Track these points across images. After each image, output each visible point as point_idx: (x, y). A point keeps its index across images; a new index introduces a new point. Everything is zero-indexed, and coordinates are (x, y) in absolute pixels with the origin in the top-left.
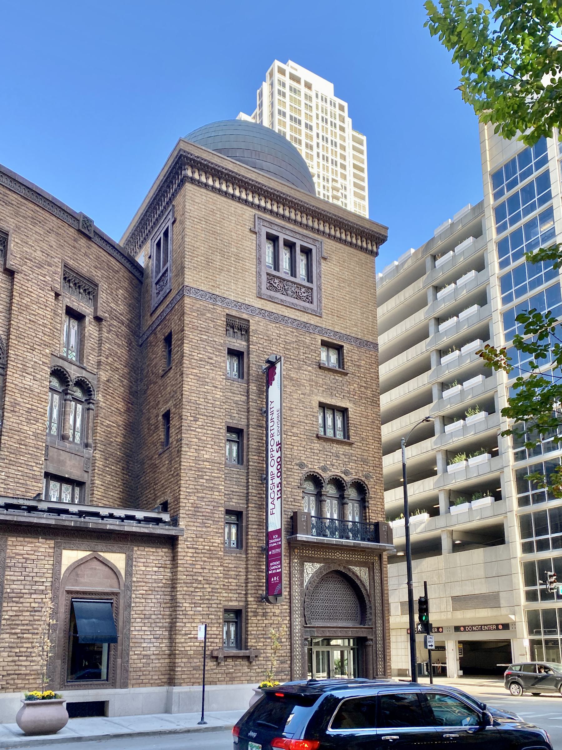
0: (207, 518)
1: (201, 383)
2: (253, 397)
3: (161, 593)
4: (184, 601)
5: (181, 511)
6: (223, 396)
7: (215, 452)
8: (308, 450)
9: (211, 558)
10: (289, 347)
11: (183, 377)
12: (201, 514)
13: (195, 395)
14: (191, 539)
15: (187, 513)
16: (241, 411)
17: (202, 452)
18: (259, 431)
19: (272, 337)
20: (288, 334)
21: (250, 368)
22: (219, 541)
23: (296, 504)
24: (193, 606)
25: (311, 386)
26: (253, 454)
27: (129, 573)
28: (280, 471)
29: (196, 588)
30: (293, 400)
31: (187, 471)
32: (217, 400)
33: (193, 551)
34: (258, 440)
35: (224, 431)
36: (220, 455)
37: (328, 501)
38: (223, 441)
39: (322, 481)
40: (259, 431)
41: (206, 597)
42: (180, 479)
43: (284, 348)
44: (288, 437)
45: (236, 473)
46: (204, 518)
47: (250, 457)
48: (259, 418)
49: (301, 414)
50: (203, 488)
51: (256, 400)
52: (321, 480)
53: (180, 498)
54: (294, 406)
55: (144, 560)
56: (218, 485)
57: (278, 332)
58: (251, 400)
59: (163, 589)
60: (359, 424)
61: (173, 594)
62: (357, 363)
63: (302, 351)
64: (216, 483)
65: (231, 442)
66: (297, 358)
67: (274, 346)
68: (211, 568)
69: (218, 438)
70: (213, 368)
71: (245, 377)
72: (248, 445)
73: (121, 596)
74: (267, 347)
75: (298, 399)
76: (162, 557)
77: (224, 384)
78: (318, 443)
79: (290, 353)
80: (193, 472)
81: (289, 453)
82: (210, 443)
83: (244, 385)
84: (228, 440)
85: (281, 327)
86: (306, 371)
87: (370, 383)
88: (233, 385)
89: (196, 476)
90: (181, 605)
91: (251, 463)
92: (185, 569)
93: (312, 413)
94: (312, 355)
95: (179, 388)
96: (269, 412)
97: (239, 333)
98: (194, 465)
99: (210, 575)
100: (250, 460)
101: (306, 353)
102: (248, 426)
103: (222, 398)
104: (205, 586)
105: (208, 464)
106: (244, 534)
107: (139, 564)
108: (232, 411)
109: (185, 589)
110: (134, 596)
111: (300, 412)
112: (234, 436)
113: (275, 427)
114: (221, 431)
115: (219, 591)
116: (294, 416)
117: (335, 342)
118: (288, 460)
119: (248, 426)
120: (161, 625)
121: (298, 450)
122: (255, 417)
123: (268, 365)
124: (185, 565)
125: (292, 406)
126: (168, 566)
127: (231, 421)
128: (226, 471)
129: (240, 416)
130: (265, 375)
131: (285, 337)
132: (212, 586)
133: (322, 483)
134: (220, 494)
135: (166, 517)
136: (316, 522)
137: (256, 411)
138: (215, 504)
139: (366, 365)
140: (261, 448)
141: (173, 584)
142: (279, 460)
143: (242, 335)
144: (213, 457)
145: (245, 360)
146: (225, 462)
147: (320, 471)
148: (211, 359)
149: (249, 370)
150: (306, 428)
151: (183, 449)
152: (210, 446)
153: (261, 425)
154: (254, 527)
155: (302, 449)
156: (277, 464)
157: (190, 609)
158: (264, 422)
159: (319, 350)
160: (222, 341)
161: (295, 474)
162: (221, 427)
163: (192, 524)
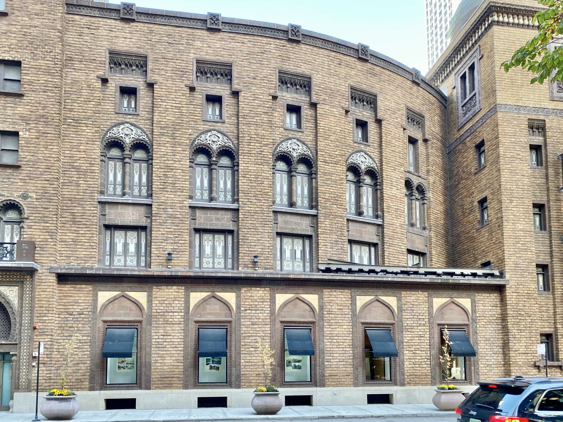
3: (495, 324)
5: (506, 268)
6: (529, 181)
7: (527, 224)
9: (529, 299)
13: (509, 184)
14: (514, 287)
17: (517, 225)
22: (534, 287)
27: (474, 311)
29: (520, 319)
33: (517, 294)
35: (531, 207)
51: (554, 181)
55: (482, 302)
59: (496, 321)
61: (504, 324)
64: (529, 245)
71: (544, 165)
72: (550, 216)
73: (471, 326)
80: (512, 240)
89: (514, 242)
97: (537, 131)
99: (529, 310)
102: (549, 201)
104: (527, 318)
107: (480, 305)
109: (513, 320)
110: (478, 326)
115: (536, 321)
119: (549, 201)
120: (497, 344)
132: (531, 318)
135: (497, 273)
137: (554, 189)
138: (529, 261)
141: (504, 318)
143: (539, 132)
145: (543, 151)
151: (504, 224)
154: (558, 275)
157: (517, 334)
160: (526, 140)
163: (514, 276)
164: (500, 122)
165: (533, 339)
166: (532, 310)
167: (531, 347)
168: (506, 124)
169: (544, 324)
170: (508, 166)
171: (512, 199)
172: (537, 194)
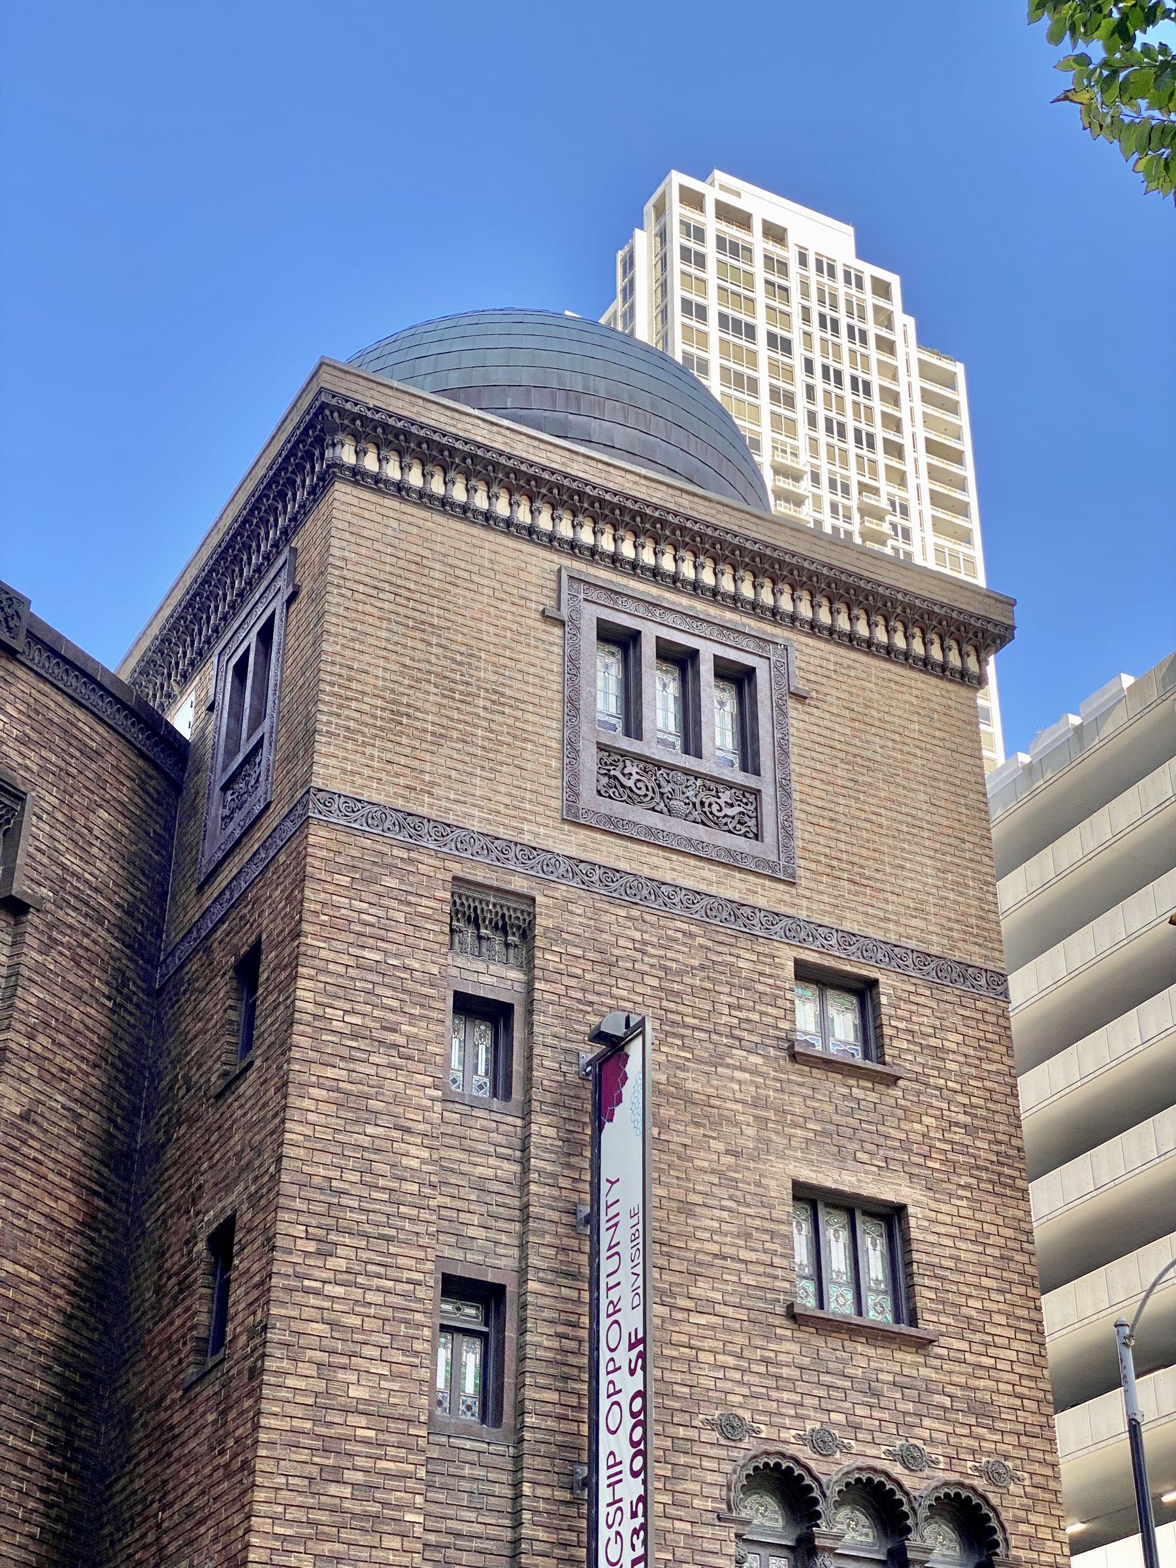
1: (350, 1115)
2: (542, 1164)
6: (433, 1162)
7: (393, 1377)
8: (755, 1368)
11: (285, 1096)
13: (328, 1159)
16: (497, 1218)
17: (341, 1375)
18: (565, 1292)
19: (616, 952)
20: (676, 940)
21: (536, 1061)
25: (762, 1122)
26: (541, 1381)
28: (640, 1449)
30: (694, 1175)
31: (279, 1452)
32: (407, 1175)
34: (561, 1329)
35: (430, 1291)
36: (412, 1387)
38: (427, 1332)
39: (816, 1494)
40: (565, 1292)
42: (253, 1485)
43: (661, 989)
45: (474, 1457)
47: (529, 1393)
48: (566, 1241)
49: (725, 1227)
50: (337, 1518)
51: (554, 1175)
52: (809, 1488)
54: (698, 1199)
56: (398, 1507)
58: (534, 1176)
60: (951, 1264)
62: (933, 1042)
63: (725, 999)
64: (392, 1497)
65: (459, 1337)
66: (705, 1025)
67: (621, 983)
69: (406, 1322)
71: (517, 1094)
72: (521, 1347)
75: (713, 1172)
77: (436, 1118)
78: (793, 1340)
79: (681, 1008)
80: (304, 1455)
81: (679, 1377)
82: (374, 1338)
83: (510, 1119)
84: (444, 1328)
85: (647, 917)
86: (742, 1069)
88: (471, 1123)
89: (315, 1471)
91: (529, 1420)
93: (768, 1225)
94: (762, 1013)
95: (272, 1133)
96: (603, 1218)
97: (498, 939)
98: (308, 1425)
100: (529, 1405)
101: (739, 1008)
102: (522, 1273)
103: (425, 1168)
105: (362, 1421)
111: (721, 1221)
112: (470, 1316)
113: (625, 1276)
114: (421, 1292)
116: (699, 1234)
117: (848, 968)
118: (677, 1405)
119: (522, 1273)
121: (716, 1366)
122: (548, 1239)
123: (599, 1048)
125: (692, 1198)
127: (459, 1255)
129: (492, 1235)
130: (590, 1086)
131: (662, 952)
133: (816, 1502)
137: (555, 1216)
139: (963, 1049)
140: (572, 1360)
143: (507, 945)
144: (384, 1395)
145: (518, 1034)
146: (431, 1415)
147: (805, 1453)
148: (394, 1031)
150: (746, 1279)
151: (270, 1364)
152: (375, 1353)
153: (573, 1269)
155: (730, 1361)
156: (629, 1422)
158: (584, 1259)
159: (789, 995)
160: (435, 970)
161: (706, 1464)
164: (314, 867)
168: (345, 881)
170: (330, 1072)
171: (333, 1237)
172: (472, 1232)
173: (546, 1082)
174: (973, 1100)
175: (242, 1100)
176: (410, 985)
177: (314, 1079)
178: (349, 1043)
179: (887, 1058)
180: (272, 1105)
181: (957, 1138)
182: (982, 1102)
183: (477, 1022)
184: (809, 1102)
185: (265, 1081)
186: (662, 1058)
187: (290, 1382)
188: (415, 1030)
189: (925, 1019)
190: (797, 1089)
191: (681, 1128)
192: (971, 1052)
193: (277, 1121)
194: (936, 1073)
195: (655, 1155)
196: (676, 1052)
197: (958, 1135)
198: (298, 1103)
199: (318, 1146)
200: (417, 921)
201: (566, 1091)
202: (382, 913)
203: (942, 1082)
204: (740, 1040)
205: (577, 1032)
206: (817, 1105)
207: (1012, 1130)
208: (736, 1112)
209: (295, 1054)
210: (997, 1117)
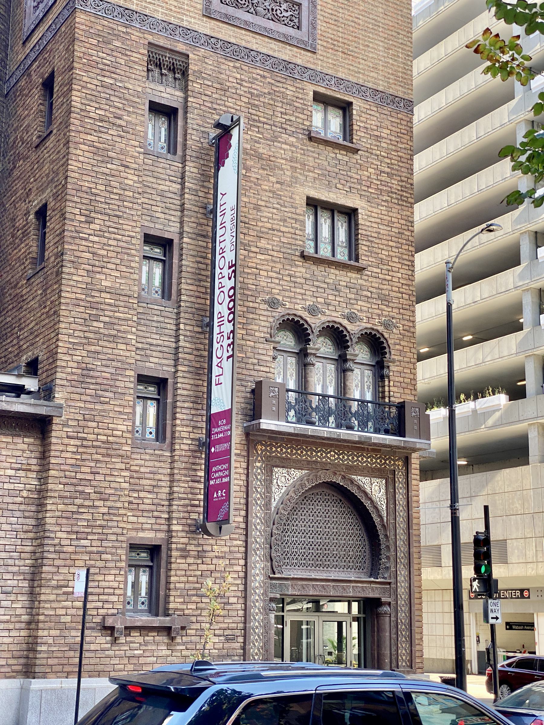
0: (103, 387)
1: (100, 159)
2: (191, 185)
3: (18, 514)
4: (58, 528)
5: (59, 375)
7: (122, 277)
8: (285, 278)
9: (108, 455)
10: (256, 102)
11: (68, 148)
12: (94, 381)
13: (89, 179)
14: (75, 423)
15: (69, 378)
16: (169, 209)
17: (98, 276)
18: (200, 243)
19: (228, 84)
20: (257, 79)
21: (188, 137)
22: (124, 428)
23: (262, 368)
24: (74, 537)
26: (189, 281)
29: (82, 506)
30: (261, 193)
31: (70, 308)
32: (127, 188)
33: (79, 443)
34: (199, 259)
35: (138, 241)
36: (131, 282)
37: (318, 365)
38: (137, 259)
39: (309, 331)
40: (200, 243)
41: (98, 523)
43: (249, 103)
44: (252, 255)
45: (158, 313)
46: (98, 387)
48: (201, 221)
49: (274, 216)
50: (97, 336)
51: (196, 191)
53: (57, 353)
54: (263, 203)
57: (238, 76)
58: (187, 190)
59: (23, 507)
60: (376, 235)
61: (40, 516)
62: (376, 133)
63: (279, 109)
64: (122, 328)
65: (152, 261)
67: (230, 100)
68: (109, 472)
69: (128, 254)
70: (122, 133)
71: (179, 152)
72: (180, 266)
74: (218, 102)
75: (270, 191)
76: (23, 451)
77: (140, 161)
79: (258, 113)
80: (82, 309)
82: (113, 260)
85: (243, 67)
86: (286, 143)
87: (397, 167)
88: (157, 164)
89: (87, 316)
90: (52, 535)
91: (183, 298)
92: (62, 474)
93: (294, 216)
94: (296, 117)
95: (63, 165)
97: (171, 75)
98: (83, 297)
99: (106, 484)
101: (286, 114)
104: (97, 503)
105: (108, 296)
106: (169, 416)
108: (154, 208)
109: (61, 507)
112: (157, 252)
114: (134, 241)
115: (122, 512)
116: (262, 219)
117: (339, 96)
118: (250, 293)
119: (181, 234)
120: (16, 569)
121: (268, 277)
122: (193, 219)
123: (218, 131)
124: (62, 467)
125: (260, 203)
126: (33, 468)
127: (152, 225)
128: (141, 310)
129: (167, 217)
130: (214, 149)
131: (250, 85)
132: (108, 504)
133: (309, 335)
134: (128, 348)
136: (296, 399)
137: (196, 209)
138: (119, 364)
139: (390, 137)
140: (203, 273)
142: (232, 292)
143: (175, 79)
144: (118, 285)
145: (180, 123)
147: (305, 315)
148: (120, 118)
149: (186, 140)
150: (283, 239)
152: (114, 267)
153: (205, 233)
154: (186, 405)
155: (274, 275)
157: (68, 542)
158: (210, 229)
159: (310, 109)
160: (140, 89)
161: (261, 318)
162: (134, 234)
163: (77, 397)
165: (109, 557)
166: (113, 485)
167: (101, 578)
169: (141, 520)
170: (89, 137)
172: (158, 215)
173: (193, 147)
174: (393, 161)
175: (48, 149)
176: (127, 96)
177: (82, 140)
178: (98, 124)
179: (354, 141)
180: (62, 152)
181: (383, 179)
182: (396, 162)
183: (161, 116)
184: (316, 160)
185: (59, 140)
186: (248, 137)
187: (75, 278)
188: (130, 119)
189: (373, 122)
190: (311, 154)
191: (256, 171)
192: (393, 138)
193: (65, 160)
194: (376, 148)
195: (243, 182)
196: (255, 134)
197: (384, 177)
198: (74, 151)
199: (85, 172)
200: (131, 64)
201: (202, 151)
202: (113, 59)
203: (379, 152)
204: (286, 129)
205: (208, 123)
206: (320, 162)
207: (409, 176)
208: (282, 164)
209: (72, 128)
210: (402, 170)
